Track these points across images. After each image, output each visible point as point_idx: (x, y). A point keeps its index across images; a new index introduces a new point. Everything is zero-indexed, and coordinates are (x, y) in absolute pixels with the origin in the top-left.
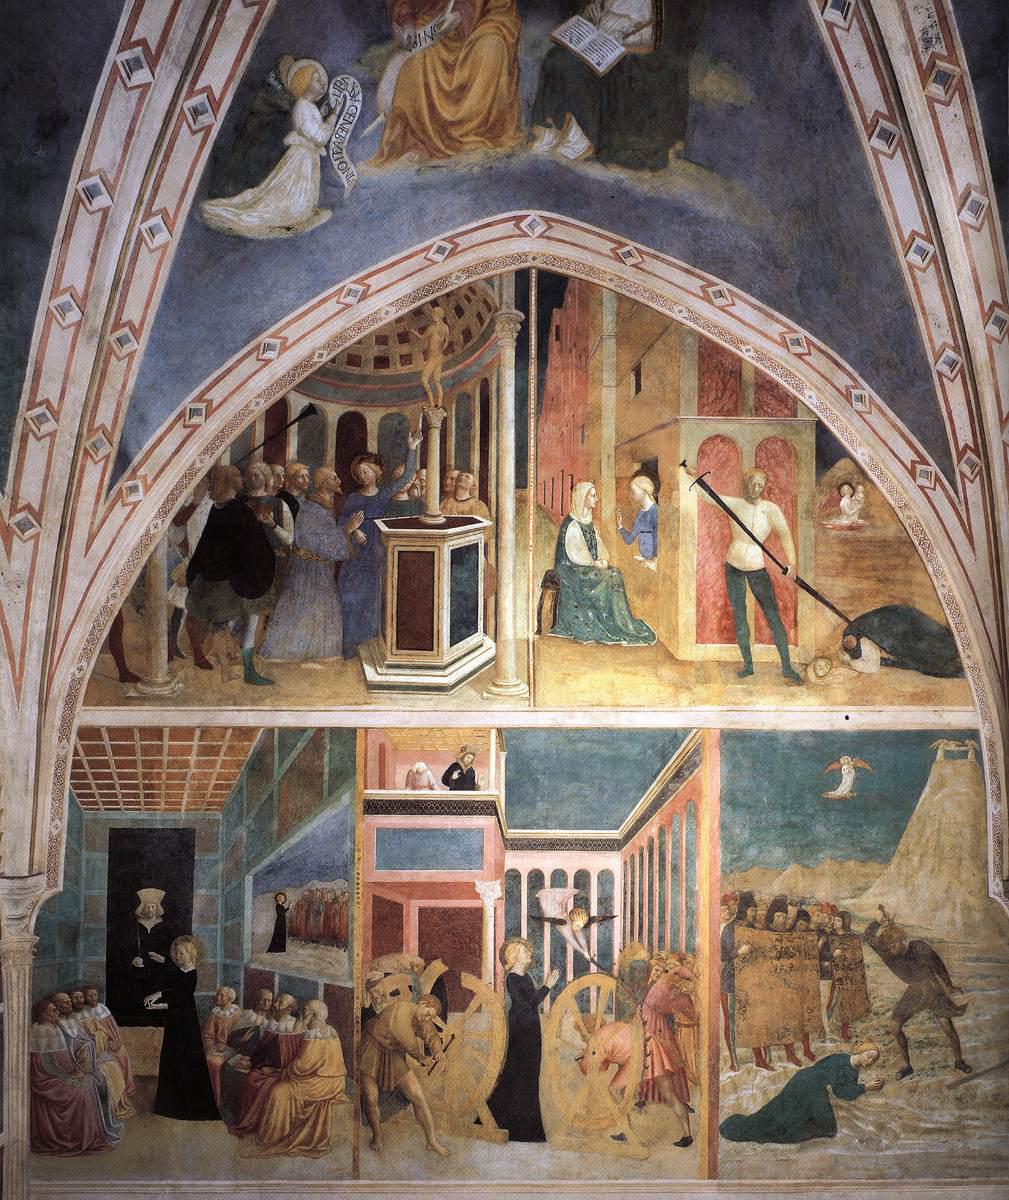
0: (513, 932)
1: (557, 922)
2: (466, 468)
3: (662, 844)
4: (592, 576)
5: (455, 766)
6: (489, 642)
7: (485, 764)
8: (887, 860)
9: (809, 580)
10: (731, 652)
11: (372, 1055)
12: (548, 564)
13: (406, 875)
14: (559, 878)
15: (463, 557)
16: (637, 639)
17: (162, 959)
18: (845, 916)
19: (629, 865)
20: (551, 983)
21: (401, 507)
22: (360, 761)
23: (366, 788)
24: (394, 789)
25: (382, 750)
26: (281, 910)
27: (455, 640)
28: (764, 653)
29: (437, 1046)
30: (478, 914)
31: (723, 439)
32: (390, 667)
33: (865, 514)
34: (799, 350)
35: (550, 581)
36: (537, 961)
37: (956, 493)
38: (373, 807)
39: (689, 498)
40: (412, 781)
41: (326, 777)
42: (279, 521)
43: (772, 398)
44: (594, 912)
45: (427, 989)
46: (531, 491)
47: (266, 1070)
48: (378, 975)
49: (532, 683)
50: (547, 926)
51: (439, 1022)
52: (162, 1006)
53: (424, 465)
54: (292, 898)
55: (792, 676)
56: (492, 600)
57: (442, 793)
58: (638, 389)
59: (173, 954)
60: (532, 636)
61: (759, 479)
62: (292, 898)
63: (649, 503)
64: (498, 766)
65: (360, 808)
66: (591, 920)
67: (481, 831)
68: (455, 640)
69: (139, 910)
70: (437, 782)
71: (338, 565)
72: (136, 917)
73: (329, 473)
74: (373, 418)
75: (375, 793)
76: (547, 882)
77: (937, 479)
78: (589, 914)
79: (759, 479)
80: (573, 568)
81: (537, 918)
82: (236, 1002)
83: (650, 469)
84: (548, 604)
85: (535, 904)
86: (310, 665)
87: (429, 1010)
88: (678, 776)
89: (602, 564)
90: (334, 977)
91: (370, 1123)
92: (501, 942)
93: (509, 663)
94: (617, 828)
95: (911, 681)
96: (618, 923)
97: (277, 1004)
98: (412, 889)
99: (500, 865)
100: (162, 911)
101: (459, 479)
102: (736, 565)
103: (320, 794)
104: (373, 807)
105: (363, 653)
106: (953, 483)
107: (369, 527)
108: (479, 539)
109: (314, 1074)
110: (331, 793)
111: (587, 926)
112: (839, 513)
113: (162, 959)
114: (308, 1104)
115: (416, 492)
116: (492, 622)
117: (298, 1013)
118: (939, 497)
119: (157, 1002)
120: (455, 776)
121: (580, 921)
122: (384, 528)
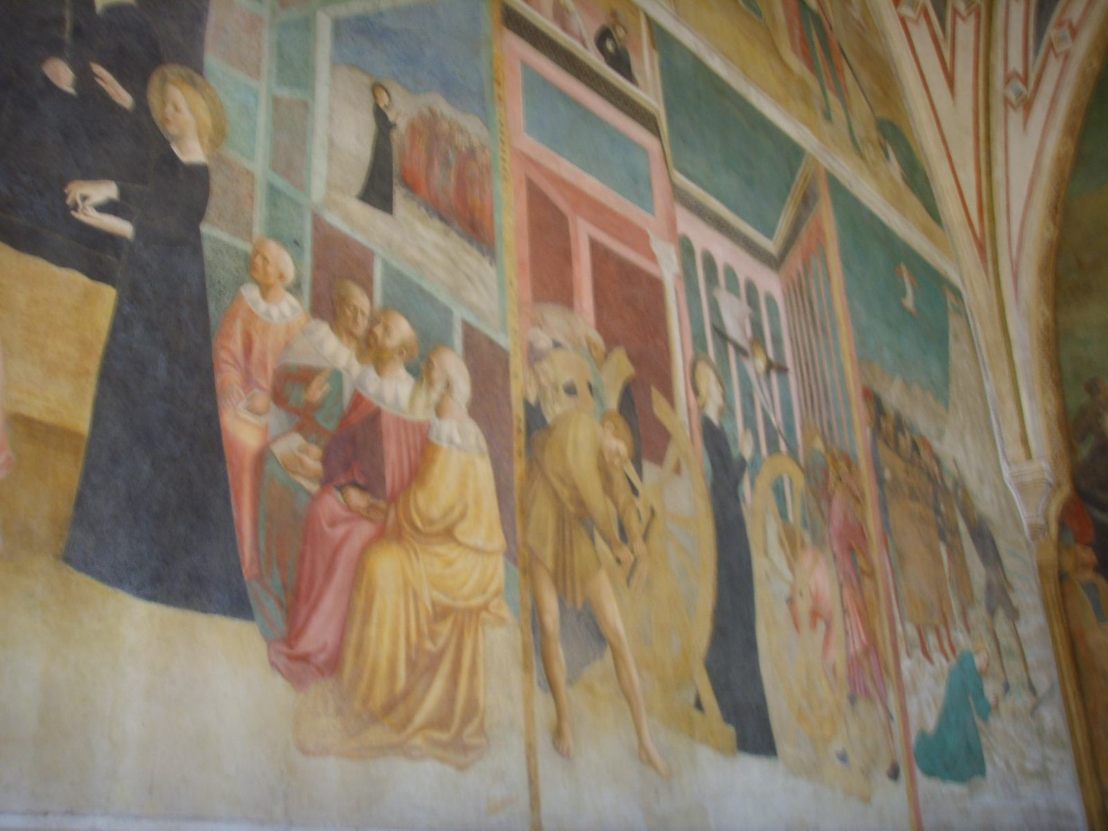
0: (699, 340)
11: (543, 511)
17: (125, 99)
20: (747, 451)
29: (635, 528)
36: (727, 409)
45: (613, 402)
47: (357, 498)
48: (543, 341)
51: (631, 470)
52: (122, 227)
59: (154, 99)
64: (652, 67)
81: (721, 334)
82: (295, 289)
87: (618, 446)
90: (472, 308)
91: (551, 686)
92: (690, 353)
97: (379, 330)
109: (448, 534)
113: (125, 99)
114: (441, 613)
117: (421, 369)
118: (921, 35)
119: (105, 208)
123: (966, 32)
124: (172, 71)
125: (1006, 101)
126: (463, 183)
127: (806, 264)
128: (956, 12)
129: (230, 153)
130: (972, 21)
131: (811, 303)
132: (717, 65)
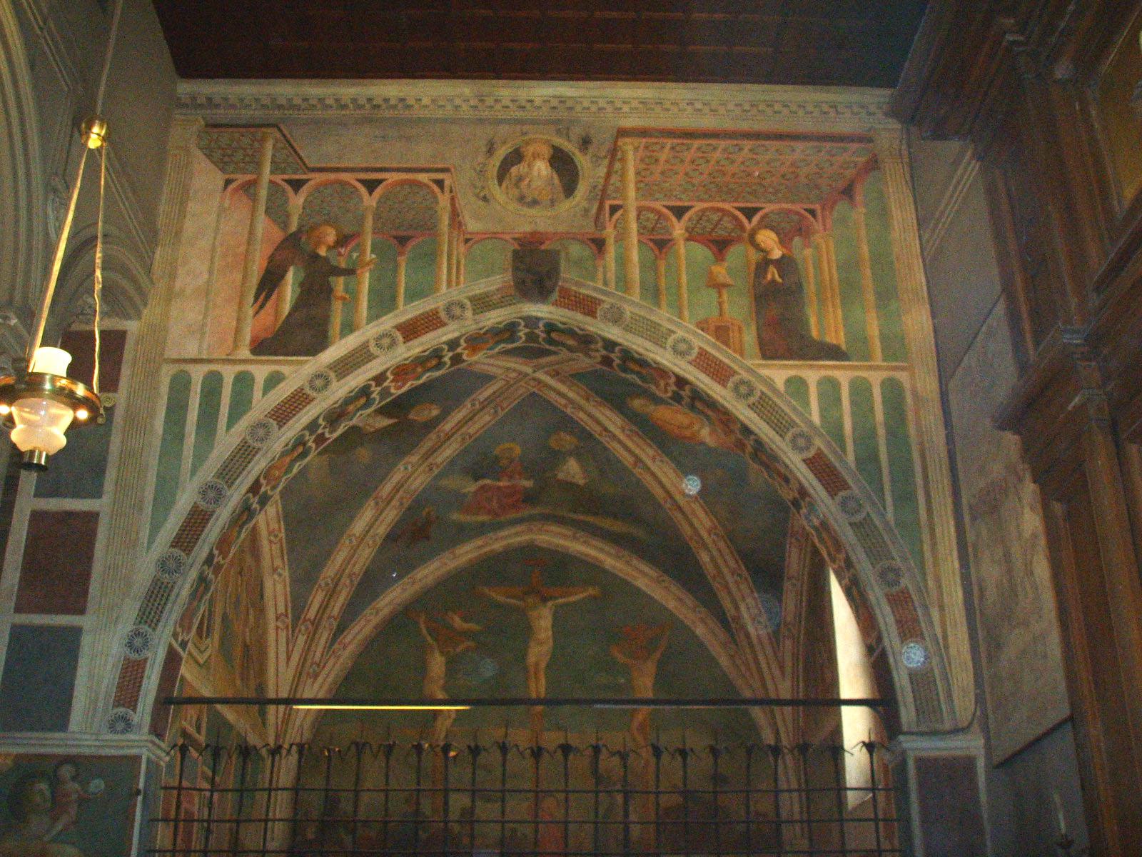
34: (272, 538)
37: (293, 636)
106: (293, 631)
118: (283, 635)
123: (301, 639)
125: (308, 674)
128: (300, 631)
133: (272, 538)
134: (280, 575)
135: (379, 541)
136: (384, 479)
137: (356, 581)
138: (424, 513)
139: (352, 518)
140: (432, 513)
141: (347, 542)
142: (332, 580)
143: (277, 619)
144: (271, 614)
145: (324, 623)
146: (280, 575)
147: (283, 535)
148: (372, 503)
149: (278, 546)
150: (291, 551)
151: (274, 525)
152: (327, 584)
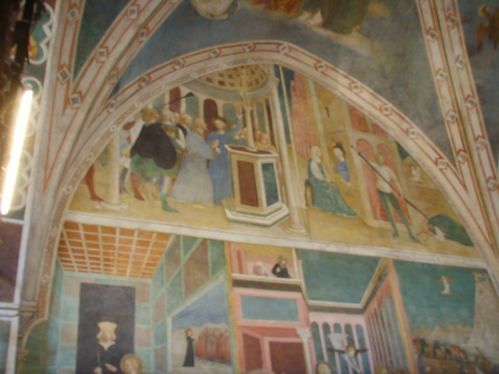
0: (320, 357)
1: (341, 352)
2: (264, 131)
3: (381, 313)
4: (325, 184)
5: (277, 266)
6: (285, 207)
7: (292, 265)
8: (472, 326)
9: (409, 199)
10: (387, 225)
12: (305, 176)
13: (260, 323)
14: (337, 327)
15: (266, 167)
16: (349, 214)
17: (113, 369)
18: (464, 352)
19: (368, 321)
21: (236, 141)
22: (228, 258)
23: (232, 272)
24: (247, 274)
25: (239, 254)
26: (190, 340)
27: (269, 203)
28: (401, 227)
30: (300, 346)
31: (365, 141)
32: (239, 212)
33: (422, 177)
34: (386, 113)
35: (308, 184)
38: (238, 283)
39: (357, 161)
40: (257, 271)
41: (210, 265)
42: (177, 136)
43: (377, 130)
44: (358, 346)
46: (293, 146)
49: (307, 227)
50: (336, 354)
53: (245, 125)
54: (196, 334)
55: (414, 239)
56: (283, 188)
57: (272, 279)
58: (328, 116)
59: (122, 366)
60: (304, 206)
61: (381, 158)
62: (196, 334)
63: (342, 159)
64: (298, 267)
65: (230, 284)
66: (357, 352)
67: (294, 300)
68: (269, 203)
69: (99, 336)
70: (269, 272)
71: (208, 161)
72: (97, 341)
73: (201, 121)
74: (220, 104)
75: (237, 276)
76: (332, 329)
77: (448, 165)
78: (355, 348)
79: (381, 158)
80: (316, 180)
81: (331, 350)
83: (339, 146)
84: (309, 194)
85: (328, 342)
86: (197, 206)
88: (380, 279)
89: (328, 180)
92: (315, 363)
93: (296, 218)
94: (358, 302)
95: (455, 245)
96: (370, 353)
98: (264, 331)
99: (307, 319)
100: (114, 337)
101: (261, 135)
102: (381, 189)
103: (207, 274)
104: (238, 283)
105: (224, 202)
107: (221, 146)
108: (274, 161)
110: (214, 273)
111: (356, 355)
112: (412, 176)
113: (113, 369)
115: (243, 136)
116: (285, 198)
118: (449, 173)
120: (278, 270)
121: (352, 353)
122: (229, 149)
123: (465, 168)
124: (126, 357)
125: (489, 189)
126: (218, 346)
127: (380, 304)
129: (144, 370)
130: (466, 163)
131: (382, 318)
132: (332, 248)
133: (386, 113)
134: (413, 133)
135: (467, 60)
136: (417, 14)
137: (476, 100)
138: (480, 14)
139: (425, 59)
140: (488, 9)
141: (439, 77)
142: (454, 111)
143: (436, 163)
144: (429, 164)
145: (473, 145)
146: (413, 133)
147: (390, 105)
148: (429, 37)
149: (394, 114)
150: (406, 112)
151: (377, 103)
152: (453, 117)
